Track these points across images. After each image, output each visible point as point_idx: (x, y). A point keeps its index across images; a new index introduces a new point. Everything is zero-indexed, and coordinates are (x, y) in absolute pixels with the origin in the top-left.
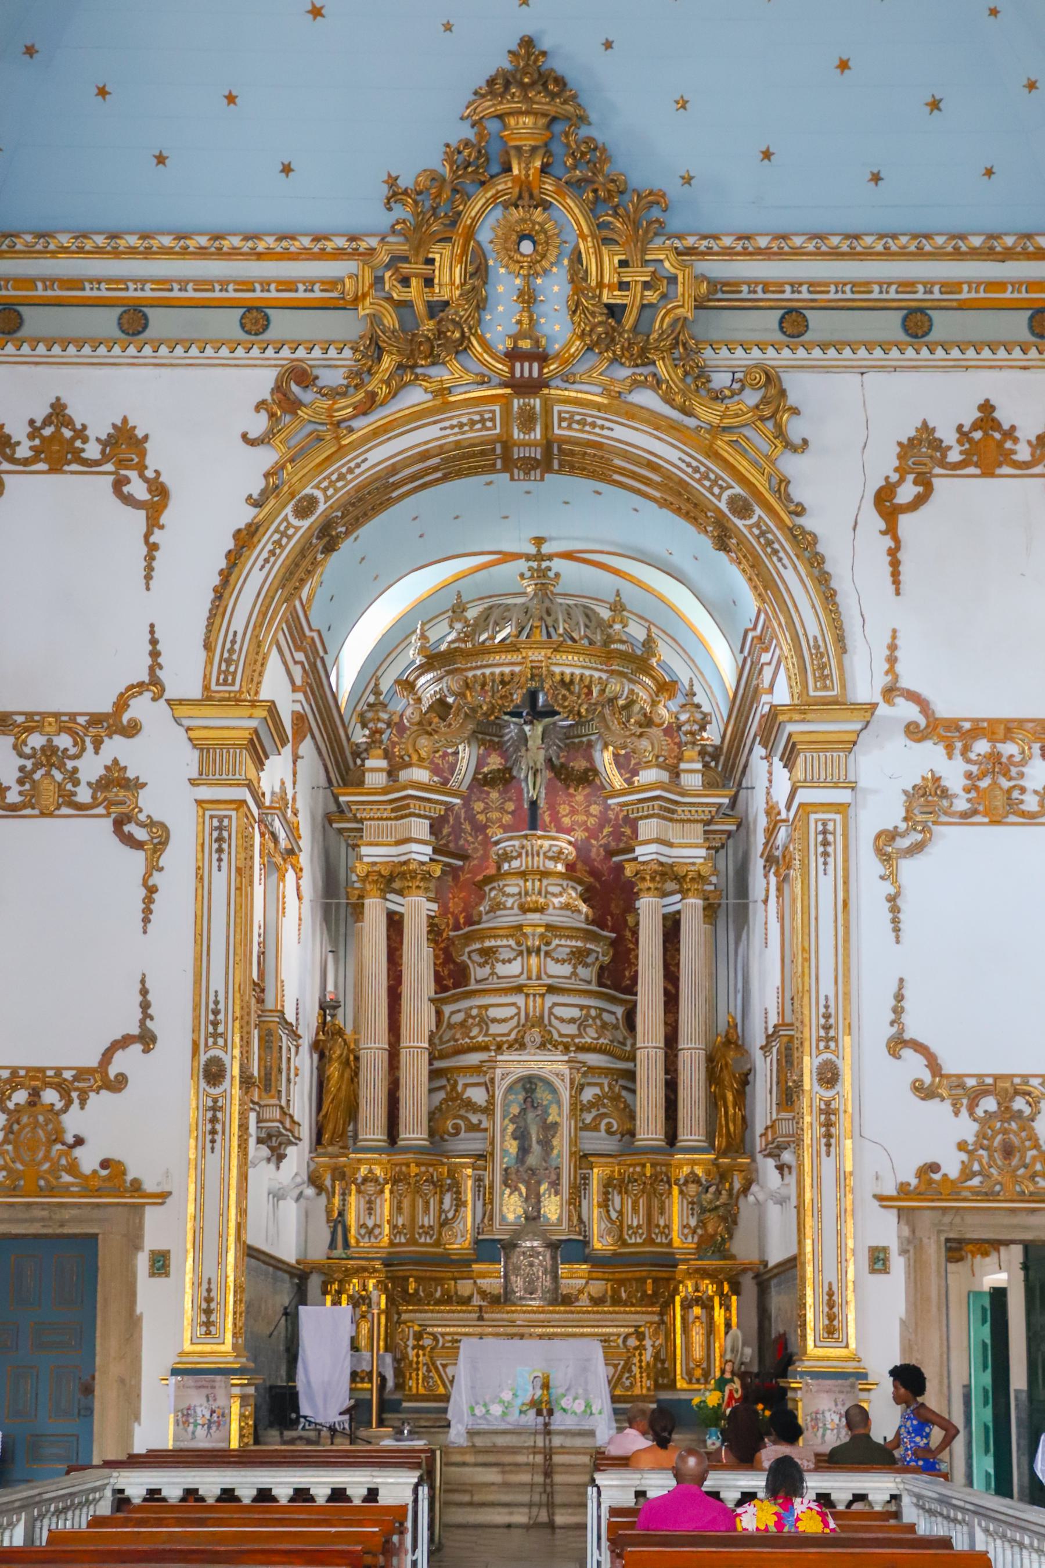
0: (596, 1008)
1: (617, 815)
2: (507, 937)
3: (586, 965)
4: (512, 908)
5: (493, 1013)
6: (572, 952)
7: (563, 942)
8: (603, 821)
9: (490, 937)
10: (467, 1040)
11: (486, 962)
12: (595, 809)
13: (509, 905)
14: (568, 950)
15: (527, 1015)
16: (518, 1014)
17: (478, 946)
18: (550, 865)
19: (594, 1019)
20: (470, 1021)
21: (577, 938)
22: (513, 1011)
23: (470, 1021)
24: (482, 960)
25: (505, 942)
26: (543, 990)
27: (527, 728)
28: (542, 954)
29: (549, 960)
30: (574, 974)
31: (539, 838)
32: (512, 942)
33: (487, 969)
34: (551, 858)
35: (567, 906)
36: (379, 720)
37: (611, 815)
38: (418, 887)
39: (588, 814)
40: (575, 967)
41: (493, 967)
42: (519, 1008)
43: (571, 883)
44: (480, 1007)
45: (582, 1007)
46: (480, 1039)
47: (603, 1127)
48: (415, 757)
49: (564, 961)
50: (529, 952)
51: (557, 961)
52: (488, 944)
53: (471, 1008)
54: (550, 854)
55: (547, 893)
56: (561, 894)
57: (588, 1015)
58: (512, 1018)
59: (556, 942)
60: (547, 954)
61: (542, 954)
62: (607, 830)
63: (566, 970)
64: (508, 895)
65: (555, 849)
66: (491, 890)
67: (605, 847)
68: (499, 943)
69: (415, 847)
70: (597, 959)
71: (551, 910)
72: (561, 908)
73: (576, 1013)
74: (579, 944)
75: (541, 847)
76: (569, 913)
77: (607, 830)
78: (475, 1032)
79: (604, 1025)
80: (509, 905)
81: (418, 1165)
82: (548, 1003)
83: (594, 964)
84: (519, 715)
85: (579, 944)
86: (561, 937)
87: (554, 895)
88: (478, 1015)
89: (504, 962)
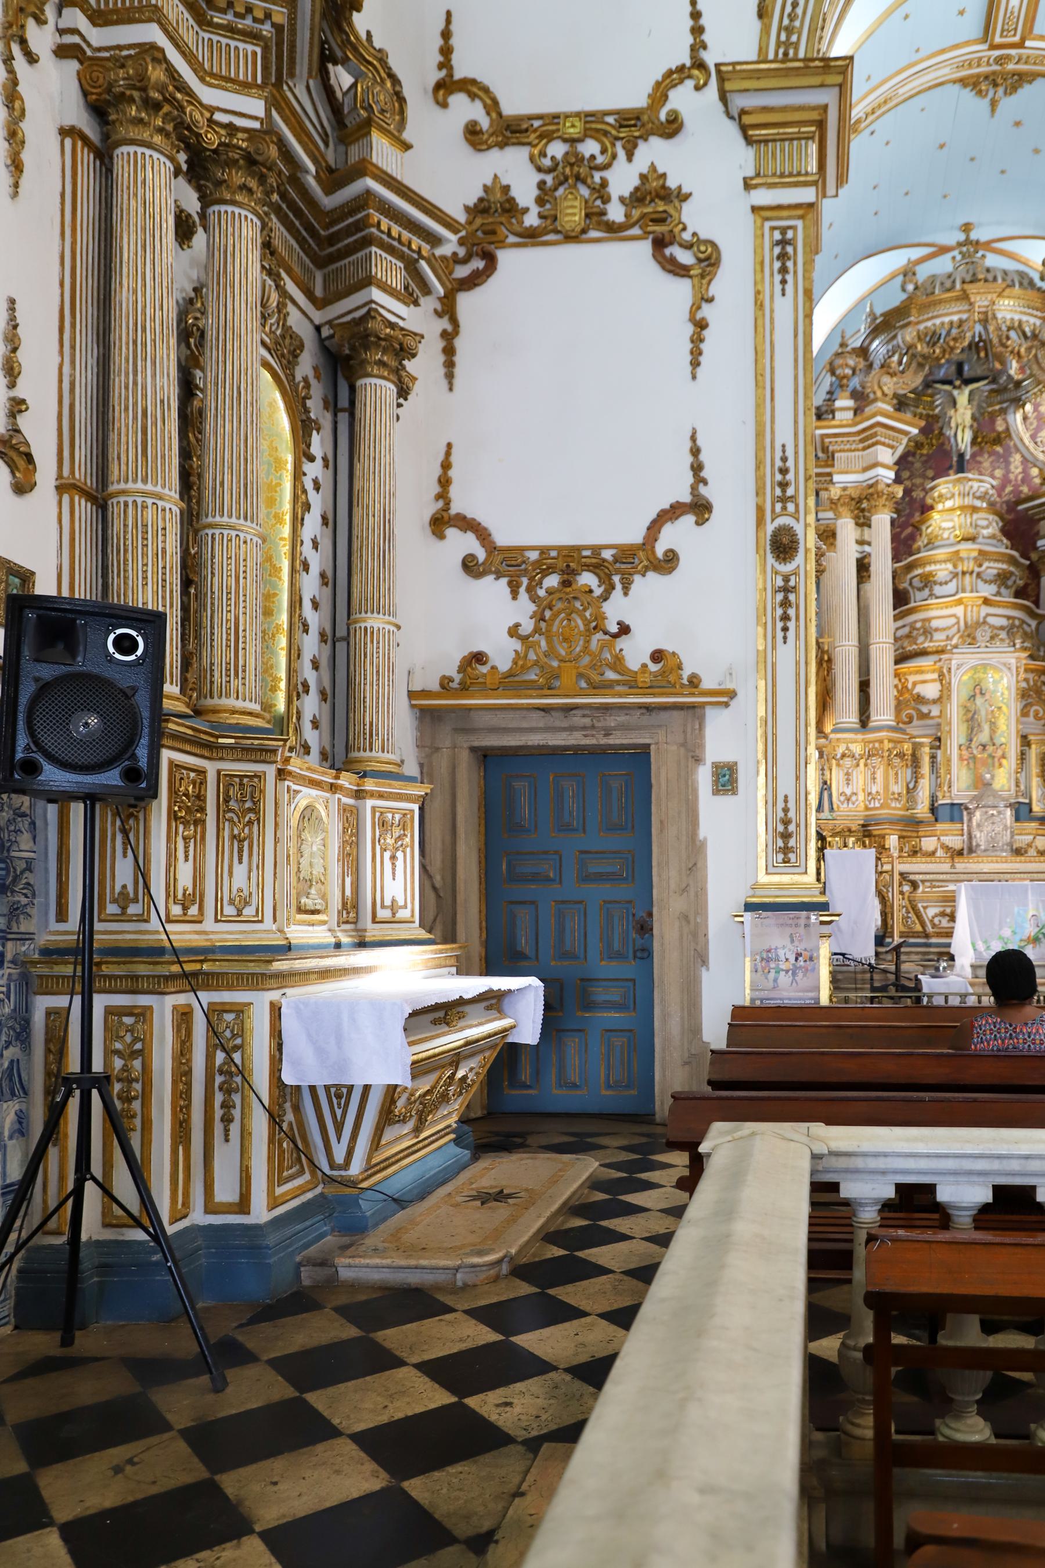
0: (1019, 619)
1: (1016, 477)
2: (945, 561)
3: (1007, 587)
4: (948, 538)
5: (934, 624)
6: (999, 575)
7: (992, 564)
8: (1005, 481)
9: (930, 563)
10: (915, 647)
11: (926, 586)
12: (998, 473)
13: (945, 535)
14: (995, 572)
15: (966, 623)
16: (958, 623)
17: (919, 571)
18: (978, 503)
19: (1018, 627)
20: (915, 632)
21: (1003, 562)
22: (953, 620)
23: (915, 632)
24: (921, 585)
25: (943, 566)
26: (980, 602)
27: (955, 392)
28: (974, 575)
29: (979, 581)
30: (998, 594)
31: (970, 480)
32: (950, 566)
33: (927, 592)
34: (979, 498)
35: (993, 537)
36: (847, 365)
37: (1012, 476)
38: (884, 505)
39: (993, 477)
40: (999, 587)
41: (931, 590)
42: (958, 618)
43: (996, 518)
44: (924, 620)
45: (1009, 618)
46: (926, 645)
47: (1032, 714)
48: (879, 394)
49: (991, 582)
50: (964, 573)
51: (986, 582)
52: (928, 568)
53: (916, 622)
54: (978, 494)
55: (976, 526)
56: (987, 527)
57: (1012, 626)
58: (953, 625)
59: (986, 564)
60: (979, 575)
61: (974, 575)
62: (1009, 489)
63: (993, 588)
64: (944, 529)
65: (982, 489)
66: (927, 528)
67: (1007, 503)
68: (938, 567)
69: (881, 471)
70: (1015, 582)
71: (980, 540)
72: (989, 538)
73: (1004, 622)
74: (1005, 566)
75: (971, 487)
76: (994, 542)
77: (1009, 489)
78: (921, 639)
79: (1025, 633)
80: (945, 535)
81: (890, 741)
82: (983, 614)
83: (1011, 587)
84: (950, 382)
85: (1005, 566)
86: (990, 560)
87: (983, 528)
88: (923, 627)
89: (941, 584)
